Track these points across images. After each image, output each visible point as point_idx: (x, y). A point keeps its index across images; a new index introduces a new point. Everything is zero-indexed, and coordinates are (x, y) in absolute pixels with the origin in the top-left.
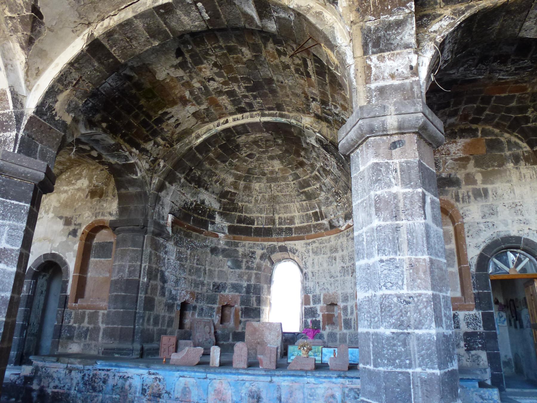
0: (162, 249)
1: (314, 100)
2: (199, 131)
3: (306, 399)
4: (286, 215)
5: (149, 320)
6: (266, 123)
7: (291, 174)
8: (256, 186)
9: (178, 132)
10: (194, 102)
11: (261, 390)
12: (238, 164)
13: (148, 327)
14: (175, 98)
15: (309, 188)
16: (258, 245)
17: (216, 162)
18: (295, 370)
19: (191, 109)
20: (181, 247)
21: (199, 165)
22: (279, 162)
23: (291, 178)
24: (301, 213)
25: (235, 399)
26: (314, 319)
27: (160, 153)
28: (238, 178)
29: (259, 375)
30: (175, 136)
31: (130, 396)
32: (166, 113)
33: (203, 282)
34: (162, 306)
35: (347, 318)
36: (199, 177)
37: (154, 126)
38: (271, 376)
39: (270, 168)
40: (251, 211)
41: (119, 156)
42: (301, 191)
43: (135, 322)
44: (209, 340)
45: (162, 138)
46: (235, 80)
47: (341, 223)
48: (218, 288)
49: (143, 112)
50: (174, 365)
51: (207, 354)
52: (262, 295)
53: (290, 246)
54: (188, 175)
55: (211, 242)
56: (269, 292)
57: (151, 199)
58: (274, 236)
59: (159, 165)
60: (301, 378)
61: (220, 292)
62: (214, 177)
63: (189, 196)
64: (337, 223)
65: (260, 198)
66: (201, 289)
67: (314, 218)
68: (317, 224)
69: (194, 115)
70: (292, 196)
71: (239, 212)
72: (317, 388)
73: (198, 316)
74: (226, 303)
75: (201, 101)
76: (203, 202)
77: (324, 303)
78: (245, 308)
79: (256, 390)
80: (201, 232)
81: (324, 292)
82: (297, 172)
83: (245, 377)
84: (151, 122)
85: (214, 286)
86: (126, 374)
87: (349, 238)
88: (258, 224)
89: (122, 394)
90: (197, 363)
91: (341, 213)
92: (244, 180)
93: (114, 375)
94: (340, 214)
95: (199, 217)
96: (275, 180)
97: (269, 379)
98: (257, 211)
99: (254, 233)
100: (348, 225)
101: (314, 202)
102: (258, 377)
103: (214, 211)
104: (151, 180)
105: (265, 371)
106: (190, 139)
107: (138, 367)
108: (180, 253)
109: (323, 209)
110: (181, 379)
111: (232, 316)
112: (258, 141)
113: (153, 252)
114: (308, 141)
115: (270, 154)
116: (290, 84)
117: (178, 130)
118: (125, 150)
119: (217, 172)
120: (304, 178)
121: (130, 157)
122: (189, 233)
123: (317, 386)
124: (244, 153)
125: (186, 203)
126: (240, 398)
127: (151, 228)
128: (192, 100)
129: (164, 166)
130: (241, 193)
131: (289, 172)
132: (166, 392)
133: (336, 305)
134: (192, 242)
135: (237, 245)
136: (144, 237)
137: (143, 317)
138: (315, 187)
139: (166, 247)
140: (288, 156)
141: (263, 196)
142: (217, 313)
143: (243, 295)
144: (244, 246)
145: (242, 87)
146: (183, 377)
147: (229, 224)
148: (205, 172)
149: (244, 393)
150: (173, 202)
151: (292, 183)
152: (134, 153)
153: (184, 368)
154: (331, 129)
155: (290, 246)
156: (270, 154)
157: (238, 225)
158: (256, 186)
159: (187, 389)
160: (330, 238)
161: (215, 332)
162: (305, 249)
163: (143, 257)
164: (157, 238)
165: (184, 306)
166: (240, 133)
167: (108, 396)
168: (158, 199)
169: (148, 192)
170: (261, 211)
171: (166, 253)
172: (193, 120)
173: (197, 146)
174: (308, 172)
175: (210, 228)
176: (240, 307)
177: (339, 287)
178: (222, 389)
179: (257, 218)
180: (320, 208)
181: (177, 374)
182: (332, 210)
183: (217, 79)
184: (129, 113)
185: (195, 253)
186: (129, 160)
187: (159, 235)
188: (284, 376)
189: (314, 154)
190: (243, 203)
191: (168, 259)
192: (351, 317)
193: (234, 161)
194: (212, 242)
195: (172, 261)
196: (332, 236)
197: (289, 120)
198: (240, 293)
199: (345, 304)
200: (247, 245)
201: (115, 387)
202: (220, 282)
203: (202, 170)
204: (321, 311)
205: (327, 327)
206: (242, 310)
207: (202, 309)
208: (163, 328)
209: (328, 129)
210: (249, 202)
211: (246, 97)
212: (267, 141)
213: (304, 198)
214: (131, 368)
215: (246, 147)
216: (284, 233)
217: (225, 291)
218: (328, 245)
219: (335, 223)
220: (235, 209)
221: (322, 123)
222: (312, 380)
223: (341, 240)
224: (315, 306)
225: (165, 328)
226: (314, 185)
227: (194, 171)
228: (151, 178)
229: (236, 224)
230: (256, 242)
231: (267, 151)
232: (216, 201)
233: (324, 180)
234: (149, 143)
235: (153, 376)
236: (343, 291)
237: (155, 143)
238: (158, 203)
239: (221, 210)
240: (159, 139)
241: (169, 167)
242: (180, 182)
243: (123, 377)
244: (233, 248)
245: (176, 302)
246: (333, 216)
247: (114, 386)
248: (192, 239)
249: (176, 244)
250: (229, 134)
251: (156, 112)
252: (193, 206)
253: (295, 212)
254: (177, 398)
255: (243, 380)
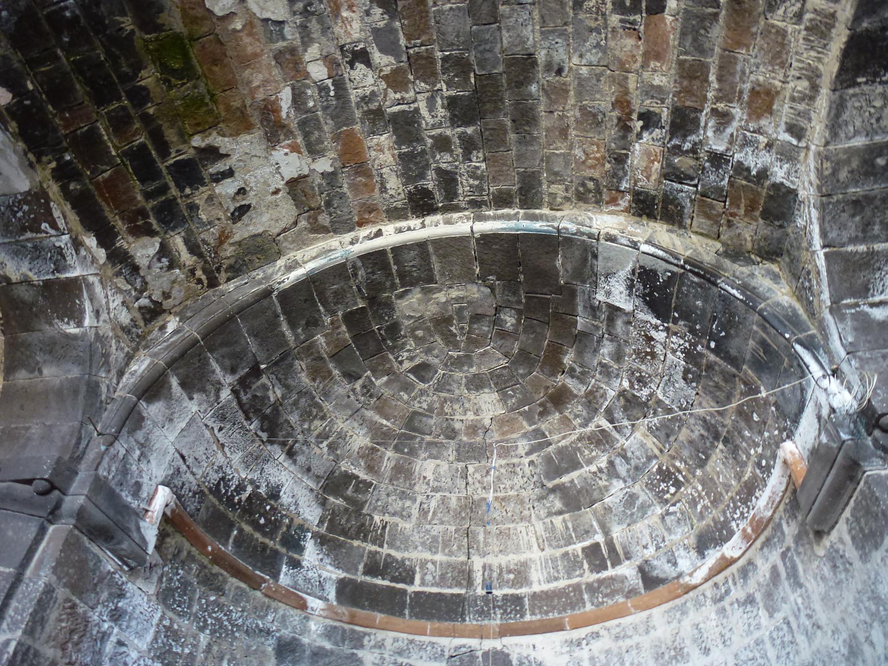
0: (104, 595)
1: (649, 120)
2: (299, 255)
4: (503, 560)
6: (487, 239)
7: (524, 435)
8: (427, 467)
9: (237, 238)
10: (299, 140)
12: (387, 392)
14: (248, 102)
15: (574, 475)
16: (421, 647)
17: (330, 372)
19: (289, 163)
20: (181, 615)
21: (282, 364)
22: (495, 396)
23: (523, 445)
24: (549, 552)
27: (174, 293)
28: (381, 436)
30: (229, 251)
32: (213, 153)
36: (276, 407)
37: (172, 184)
39: (470, 416)
40: (407, 543)
41: (37, 253)
42: (550, 485)
45: (186, 242)
46: (422, 66)
47: (685, 563)
49: (146, 119)
53: (518, 650)
54: (244, 384)
55: (281, 621)
57: (109, 417)
58: (471, 621)
59: (163, 328)
62: (317, 423)
63: (236, 458)
64: (667, 567)
65: (433, 504)
67: (589, 563)
68: (601, 582)
69: (296, 186)
70: (522, 502)
71: (374, 543)
75: (320, 141)
76: (274, 494)
80: (255, 584)
82: (543, 427)
84: (162, 167)
87: (726, 603)
88: (423, 583)
91: (682, 535)
92: (397, 449)
94: (676, 537)
95: (257, 535)
96: (479, 452)
98: (423, 544)
99: (412, 608)
100: (723, 557)
101: (588, 516)
103: (303, 529)
104: (127, 364)
106: (270, 271)
108: (171, 633)
109: (618, 532)
112: (448, 321)
113: (61, 593)
114: (600, 297)
115: (473, 370)
116: (584, 71)
117: (241, 232)
118: (61, 223)
119: (328, 406)
120: (563, 443)
121: (71, 258)
122: (216, 575)
124: (407, 358)
125: (223, 479)
127: (76, 497)
128: (294, 126)
129: (176, 332)
130: (384, 486)
131: (522, 427)
134: (221, 607)
135: (357, 641)
136: (42, 531)
138: (593, 468)
139: (121, 595)
140: (523, 376)
141: (444, 499)
144: (380, 645)
145: (439, 101)
147: (342, 574)
148: (294, 397)
150: (183, 457)
151: (526, 461)
152: (88, 249)
154: (679, 235)
155: (518, 650)
156: (473, 370)
157: (368, 579)
158: (427, 467)
160: (649, 617)
162: (566, 658)
163: (14, 604)
164: (95, 549)
166: (408, 281)
168: (132, 419)
169: (104, 389)
170: (432, 547)
171: (117, 616)
172: (287, 210)
173: (285, 291)
174: (579, 420)
175: (285, 578)
179: (423, 564)
180: (606, 532)
182: (647, 532)
183: (377, 57)
184: (101, 96)
185: (225, 646)
186: (65, 268)
187: (102, 534)
189: (607, 349)
190: (387, 518)
191: (120, 643)
193: (378, 383)
194: (284, 620)
195: (134, 655)
196: (657, 612)
197: (556, 224)
200: (388, 643)
203: (287, 387)
209: (673, 236)
210: (404, 515)
211: (443, 144)
212: (477, 318)
213: (558, 505)
215: (416, 338)
216: (499, 612)
218: (645, 641)
219: (662, 568)
220: (363, 531)
221: (651, 224)
223: (693, 616)
226: (589, 462)
227: (264, 380)
228: (129, 358)
229: (360, 578)
230: (417, 638)
231: (467, 360)
232: (311, 496)
233: (622, 441)
234: (146, 240)
237: (164, 251)
238: (131, 432)
239: (323, 530)
240: (178, 242)
241: (192, 330)
242: (218, 396)
244: (346, 649)
246: (652, 550)
248: (223, 600)
249: (165, 596)
250: (378, 276)
251: (184, 137)
252: (245, 496)
253: (530, 549)
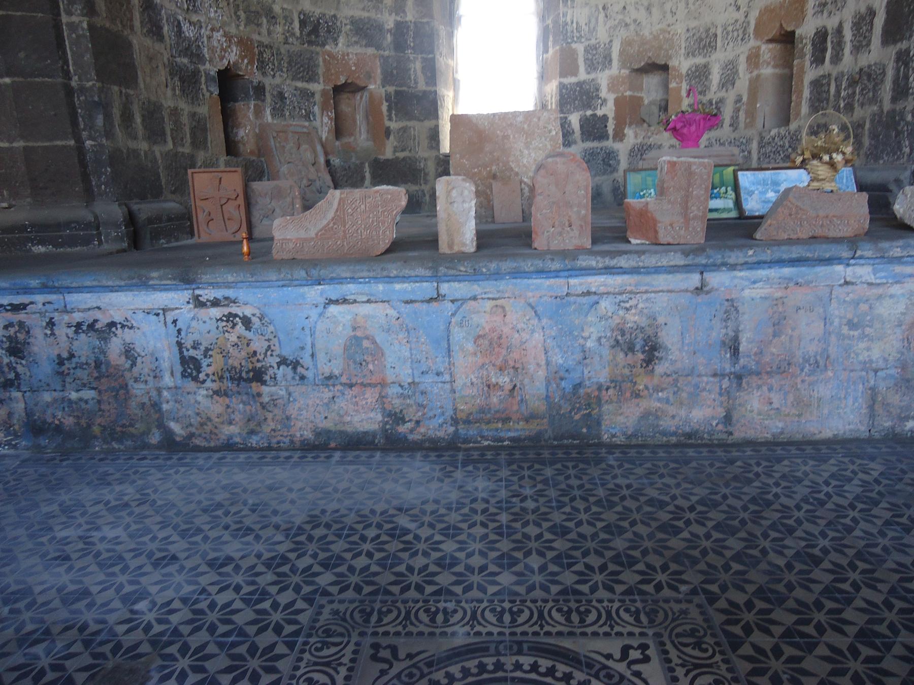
3: (833, 338)
5: (127, 118)
11: (661, 320)
13: (132, 144)
18: (790, 242)
25: (558, 359)
26: (589, 113)
29: (657, 270)
31: (138, 390)
33: (270, 10)
34: (163, 75)
35: (705, 99)
38: (702, 270)
43: (74, 123)
44: (318, 184)
48: (315, 30)
50: (293, 262)
51: (421, 204)
52: (438, 56)
56: (451, 51)
60: (821, 270)
61: (323, 45)
66: (269, 33)
72: (880, 297)
73: (273, 116)
74: (342, 80)
77: (623, 65)
78: (397, 92)
79: (643, 322)
81: (623, 33)
83: (595, 282)
85: (303, 23)
86: (98, 315)
89: (105, 384)
90: (384, 245)
93: (51, 324)
97: (695, 279)
102: (647, 279)
105: (686, 254)
107: (144, 285)
110: (333, 309)
111: (360, 117)
123: (880, 291)
126: (578, 356)
132: (283, 362)
133: (665, 68)
137: (104, 106)
142: (324, 109)
143: (387, 53)
146: (345, 301)
149: (594, 337)
153: (343, 271)
159: (366, 344)
161: (328, 162)
165: (228, 81)
167: (47, 397)
176: (383, 90)
177: (681, 12)
178: (506, 330)
181: (314, 293)
188: (759, 264)
192: (722, 94)
198: (378, 47)
199: (699, 60)
201: (67, 365)
202: (318, 12)
204: (612, 88)
205: (629, 132)
206: (388, 98)
207: (281, 96)
208: (180, 149)
214: (112, 289)
217: (335, 40)
222: (863, 272)
224: (592, 76)
225: (187, 149)
235: (216, 312)
236: (693, 24)
243: (91, 326)
245: (202, 68)
247: (61, 362)
254: (329, 378)
255: (588, 293)
